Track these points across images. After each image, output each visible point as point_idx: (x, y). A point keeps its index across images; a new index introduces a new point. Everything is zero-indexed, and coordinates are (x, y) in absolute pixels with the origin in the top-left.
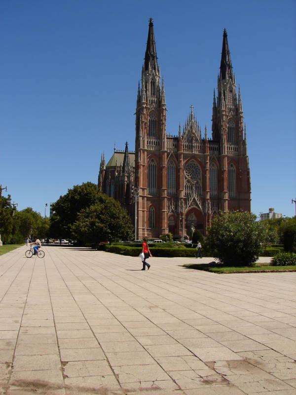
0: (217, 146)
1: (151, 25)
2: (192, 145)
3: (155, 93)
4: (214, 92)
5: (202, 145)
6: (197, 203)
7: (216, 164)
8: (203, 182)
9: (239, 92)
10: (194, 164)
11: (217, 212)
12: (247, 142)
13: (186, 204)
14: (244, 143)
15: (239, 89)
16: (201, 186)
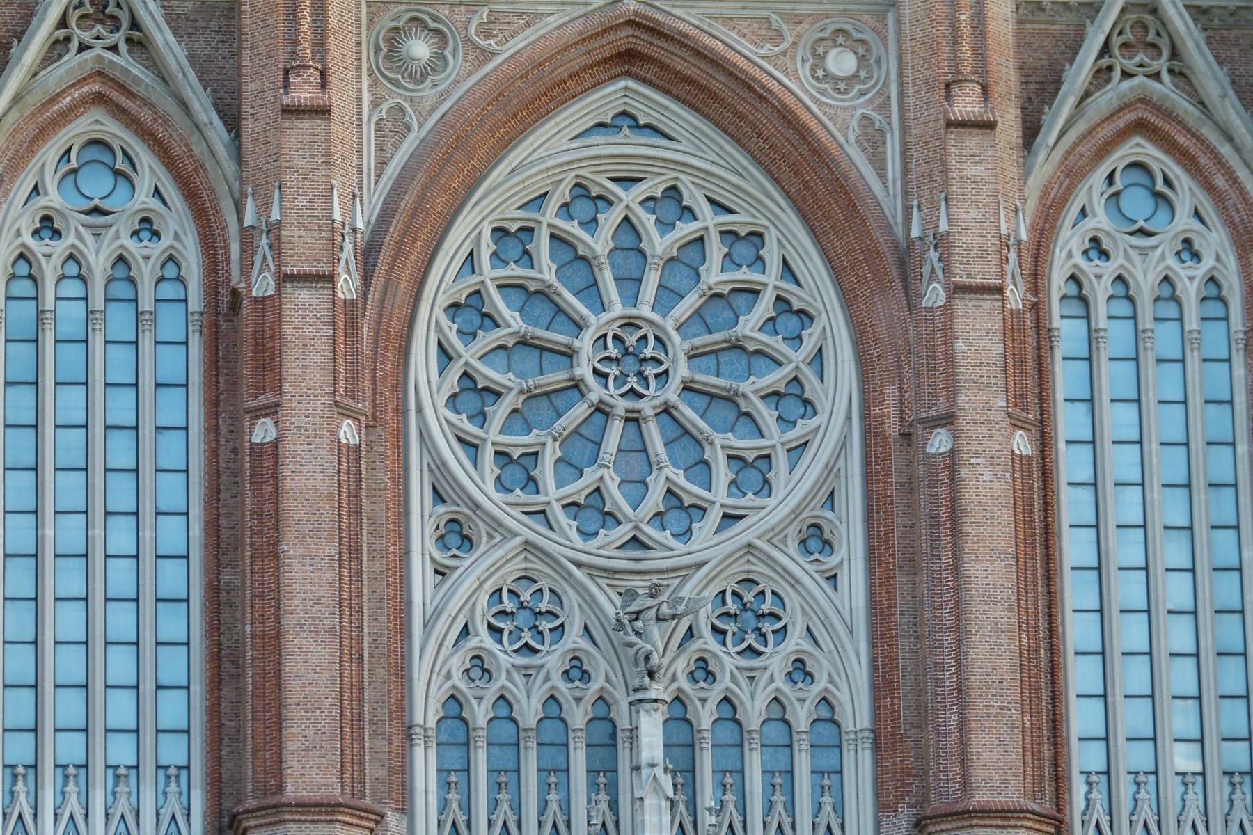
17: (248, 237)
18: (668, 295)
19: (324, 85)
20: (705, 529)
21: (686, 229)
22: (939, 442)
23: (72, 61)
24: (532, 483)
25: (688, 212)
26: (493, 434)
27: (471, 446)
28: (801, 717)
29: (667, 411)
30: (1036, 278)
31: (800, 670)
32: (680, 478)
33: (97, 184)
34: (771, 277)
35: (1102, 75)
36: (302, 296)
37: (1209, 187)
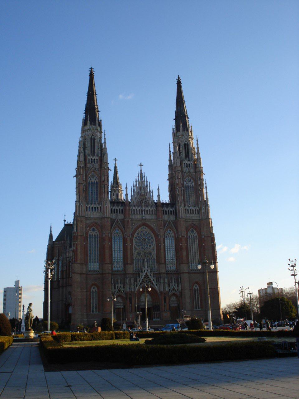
0: (172, 209)
1: (91, 75)
2: (142, 210)
3: (96, 151)
4: (170, 148)
5: (155, 208)
6: (150, 279)
7: (173, 230)
8: (157, 254)
9: (197, 144)
10: (146, 232)
11: (176, 288)
12: (210, 202)
13: (137, 282)
14: (206, 204)
15: (197, 140)
16: (155, 258)
17: (125, 235)
18: (146, 237)
19: (129, 226)
20: (148, 249)
21: (147, 233)
22: (160, 245)
23: (116, 225)
24: (139, 247)
25: (147, 233)
26: (137, 244)
27: (136, 245)
28: (153, 259)
29: (146, 243)
30: (164, 236)
31: (153, 256)
32: (146, 246)
33: (117, 231)
34: (151, 236)
35: (167, 225)
36: (128, 238)
37: (173, 231)
